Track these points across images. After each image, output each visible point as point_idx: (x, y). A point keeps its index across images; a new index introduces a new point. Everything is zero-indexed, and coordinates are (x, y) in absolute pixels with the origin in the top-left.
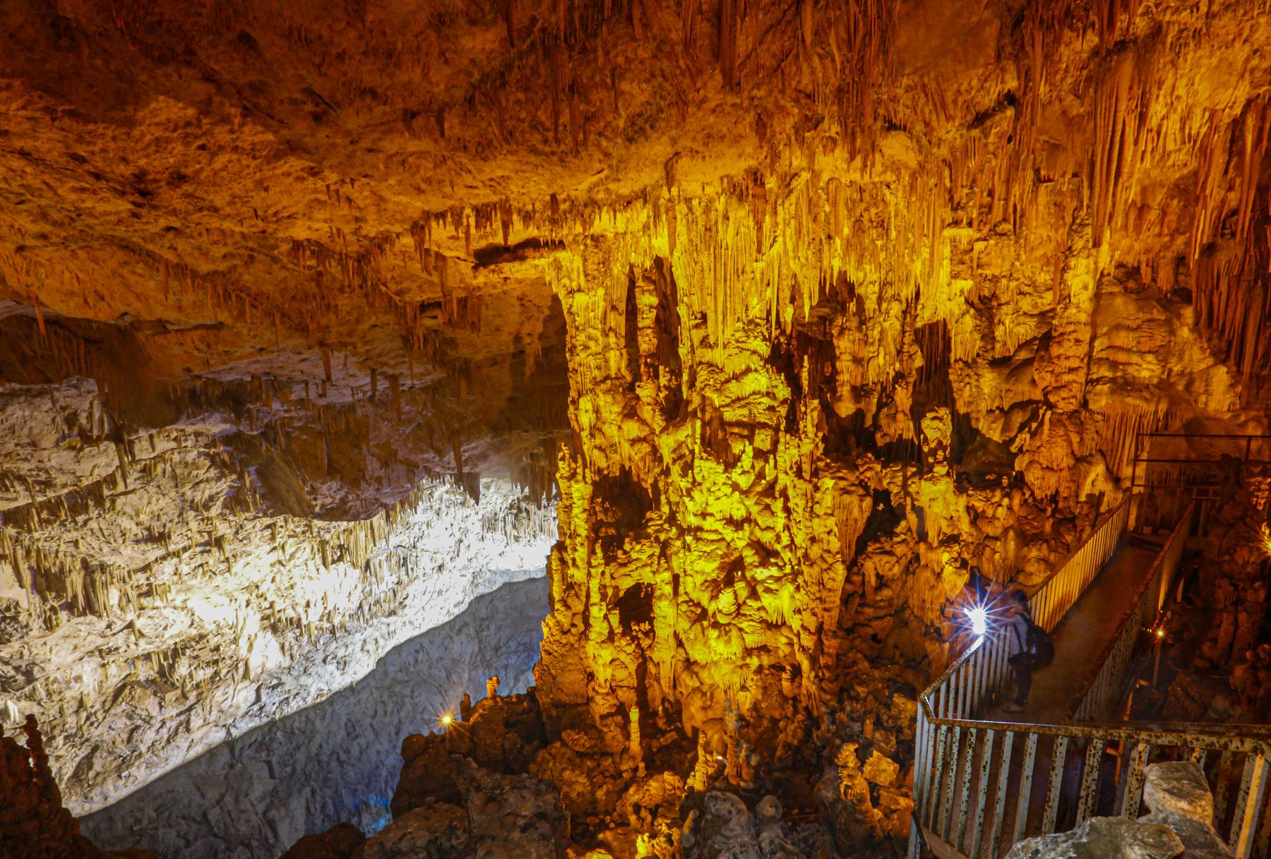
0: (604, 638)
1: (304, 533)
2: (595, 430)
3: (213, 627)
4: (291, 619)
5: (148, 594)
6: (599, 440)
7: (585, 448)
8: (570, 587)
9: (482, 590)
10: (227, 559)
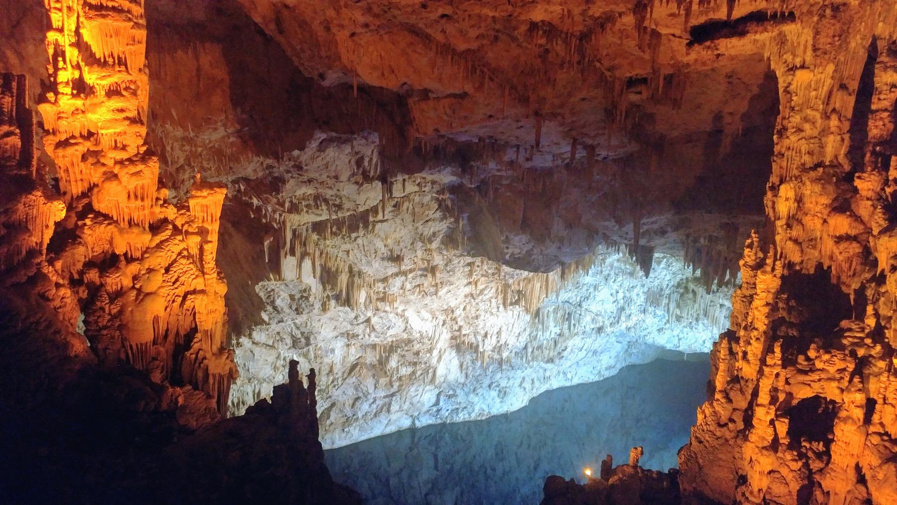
0: (766, 444)
1: (493, 274)
3: (418, 335)
4: (472, 344)
5: (383, 299)
7: (778, 238)
8: (735, 379)
9: (634, 360)
10: (436, 285)
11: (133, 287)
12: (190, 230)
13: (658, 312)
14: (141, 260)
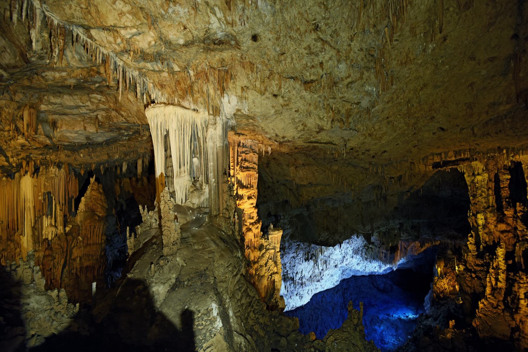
2: (485, 226)
6: (487, 230)
9: (345, 277)
11: (256, 274)
12: (270, 248)
13: (358, 257)
14: (257, 262)
